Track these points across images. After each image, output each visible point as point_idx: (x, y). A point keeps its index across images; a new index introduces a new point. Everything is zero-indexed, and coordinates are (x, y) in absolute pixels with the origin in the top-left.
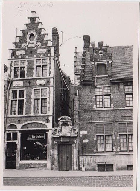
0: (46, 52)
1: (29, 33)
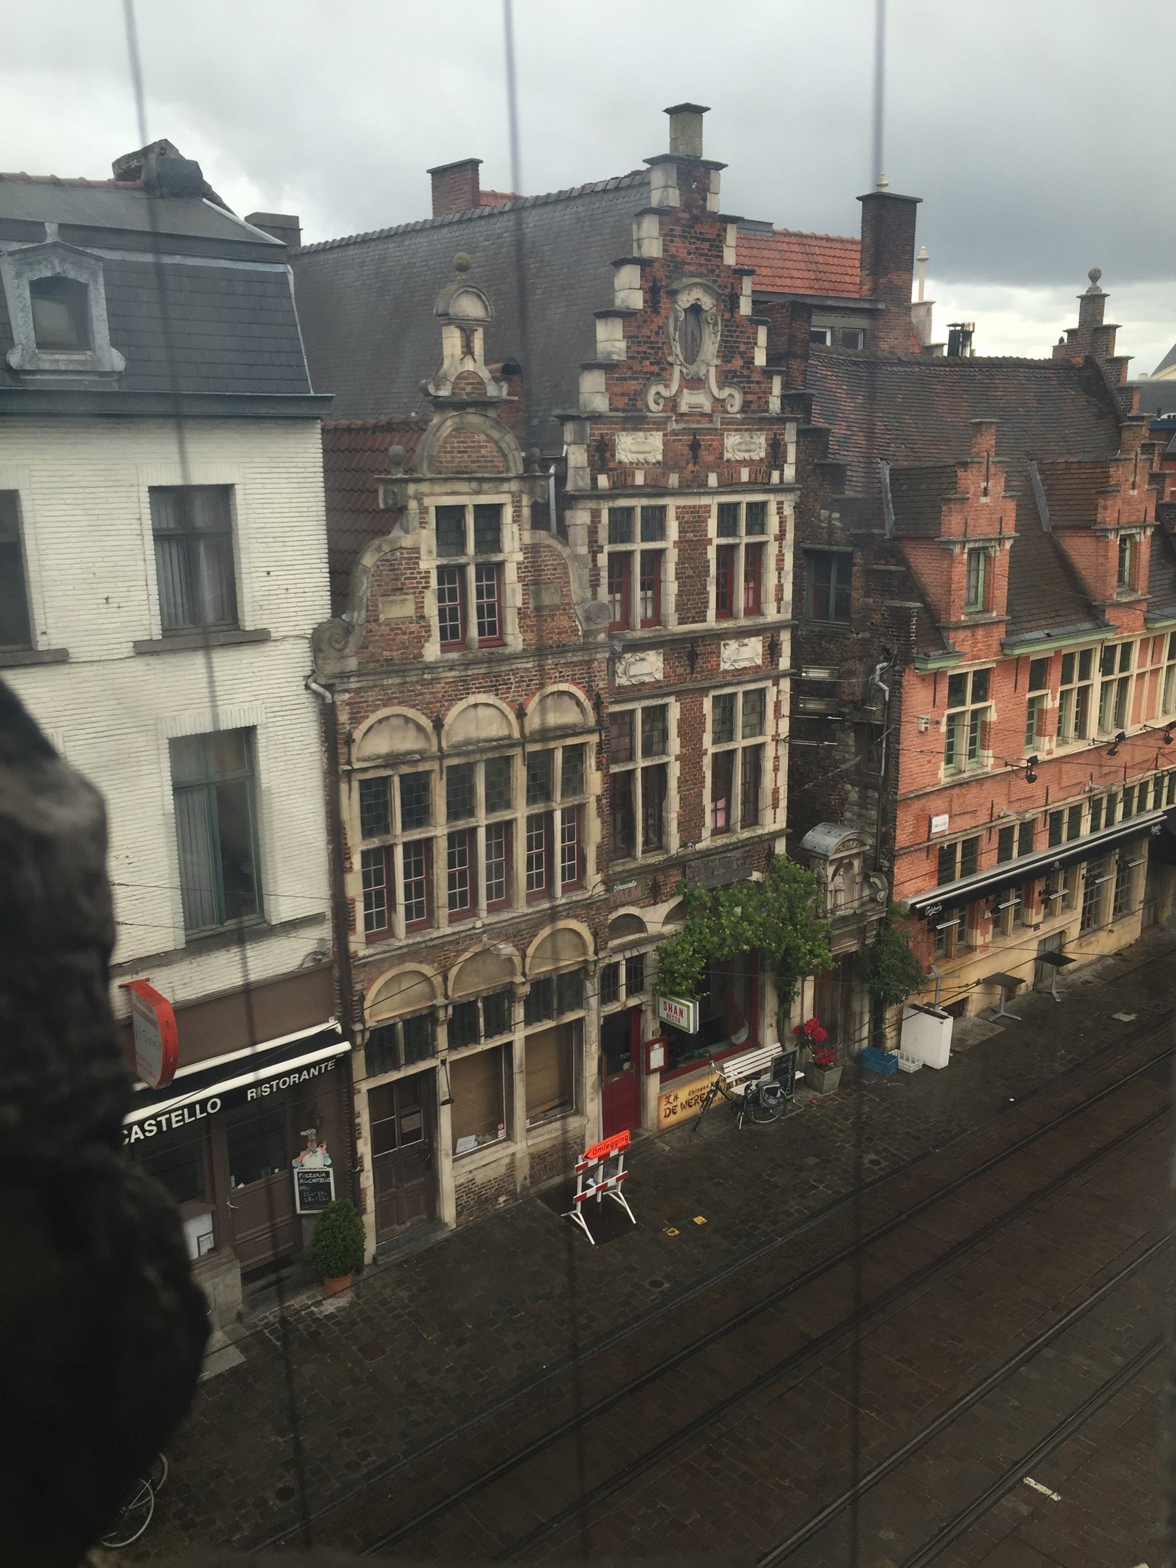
0: (763, 455)
1: (685, 300)
